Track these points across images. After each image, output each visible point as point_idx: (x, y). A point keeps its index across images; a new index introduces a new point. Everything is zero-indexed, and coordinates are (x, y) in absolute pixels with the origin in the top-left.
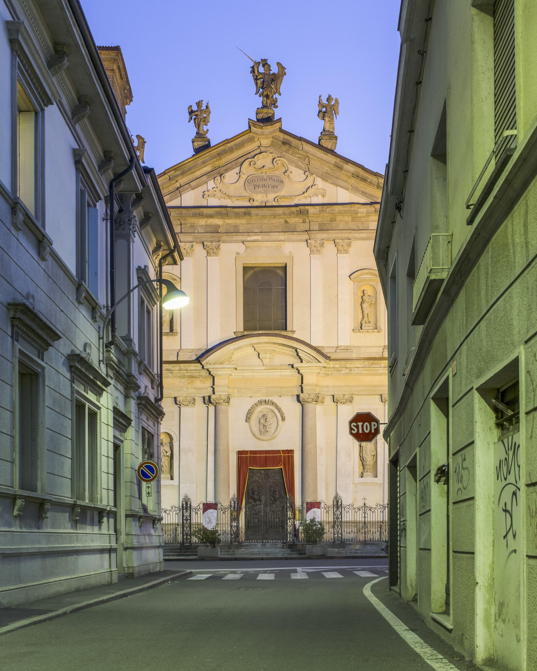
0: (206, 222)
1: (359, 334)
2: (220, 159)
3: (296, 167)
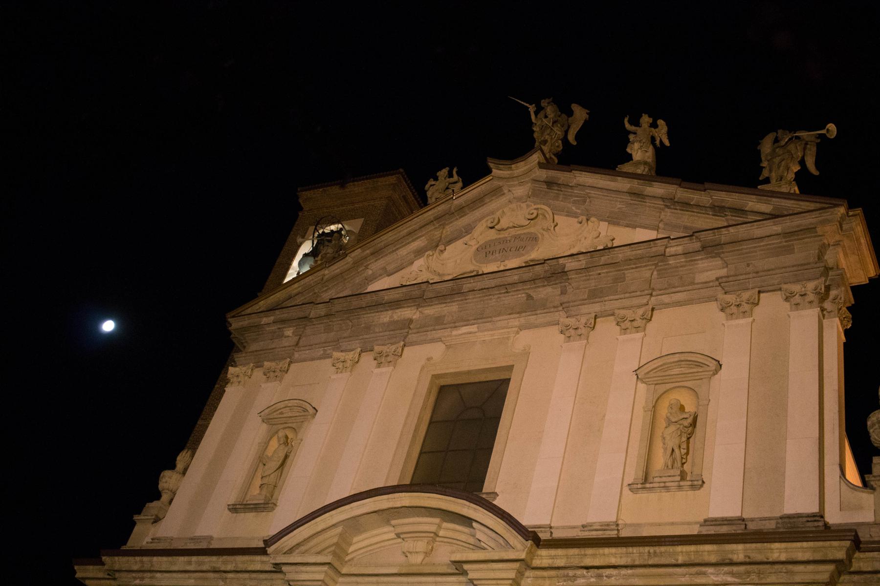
0: (391, 317)
1: (644, 495)
2: (443, 226)
3: (567, 216)
